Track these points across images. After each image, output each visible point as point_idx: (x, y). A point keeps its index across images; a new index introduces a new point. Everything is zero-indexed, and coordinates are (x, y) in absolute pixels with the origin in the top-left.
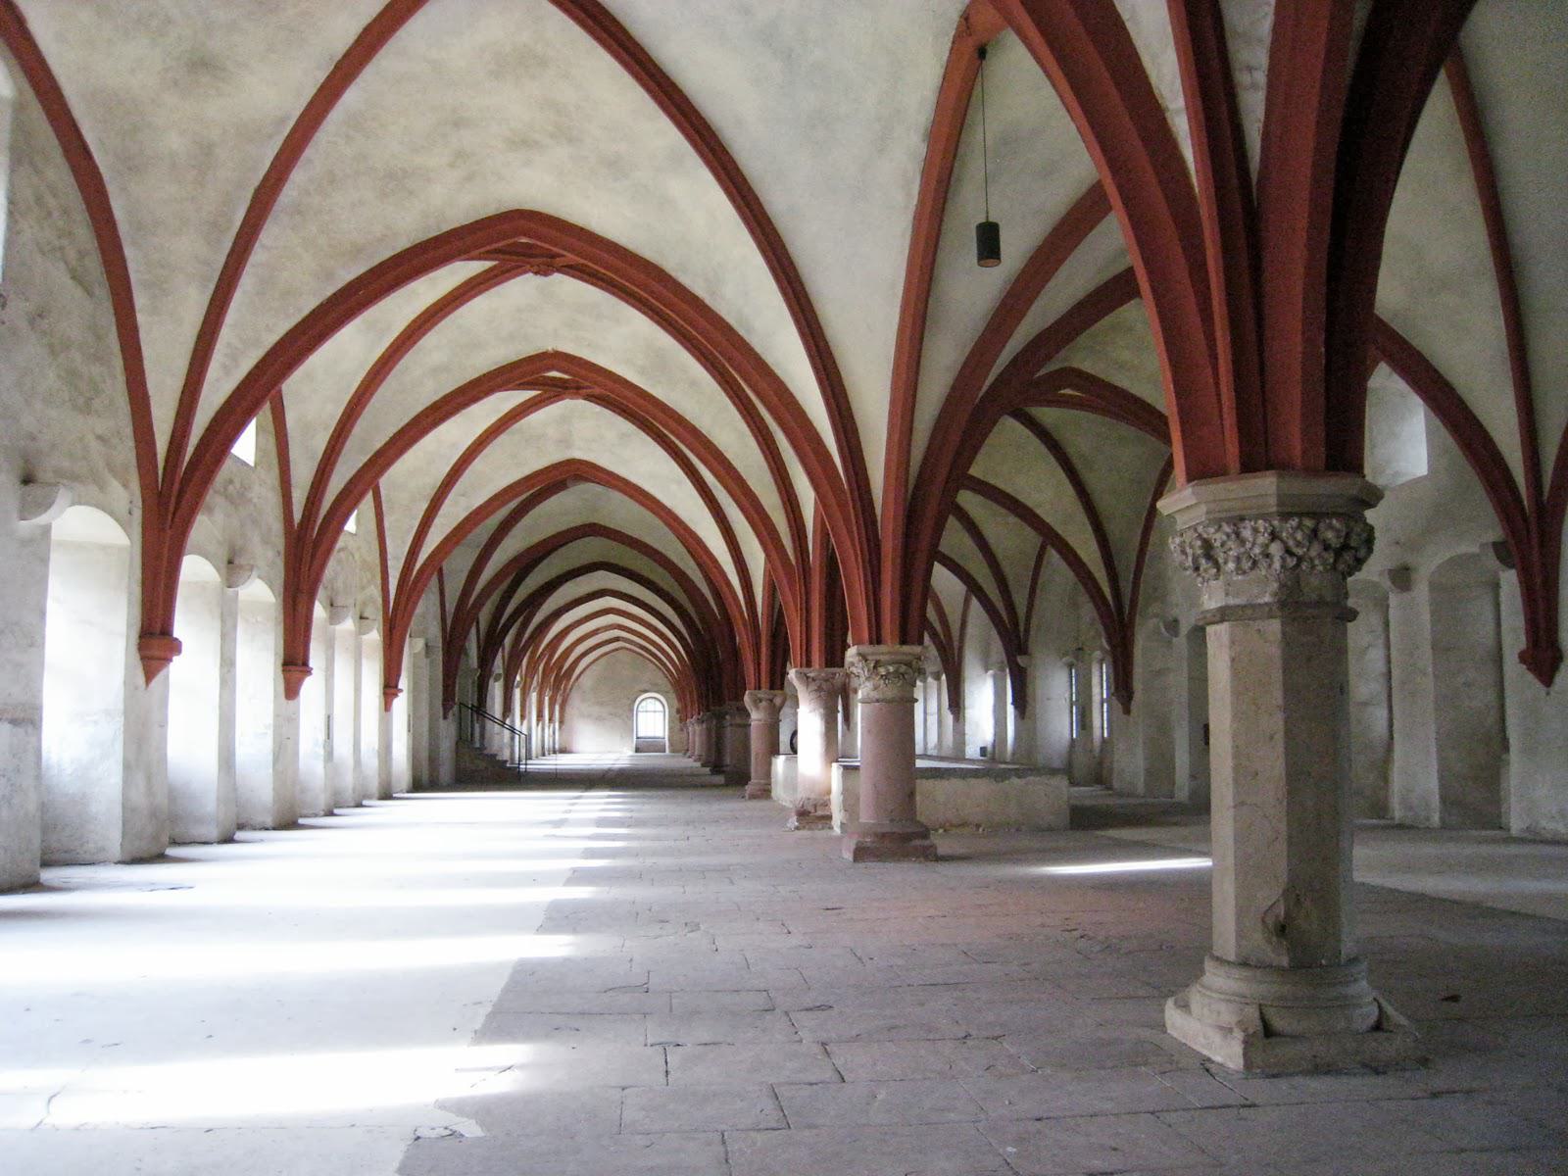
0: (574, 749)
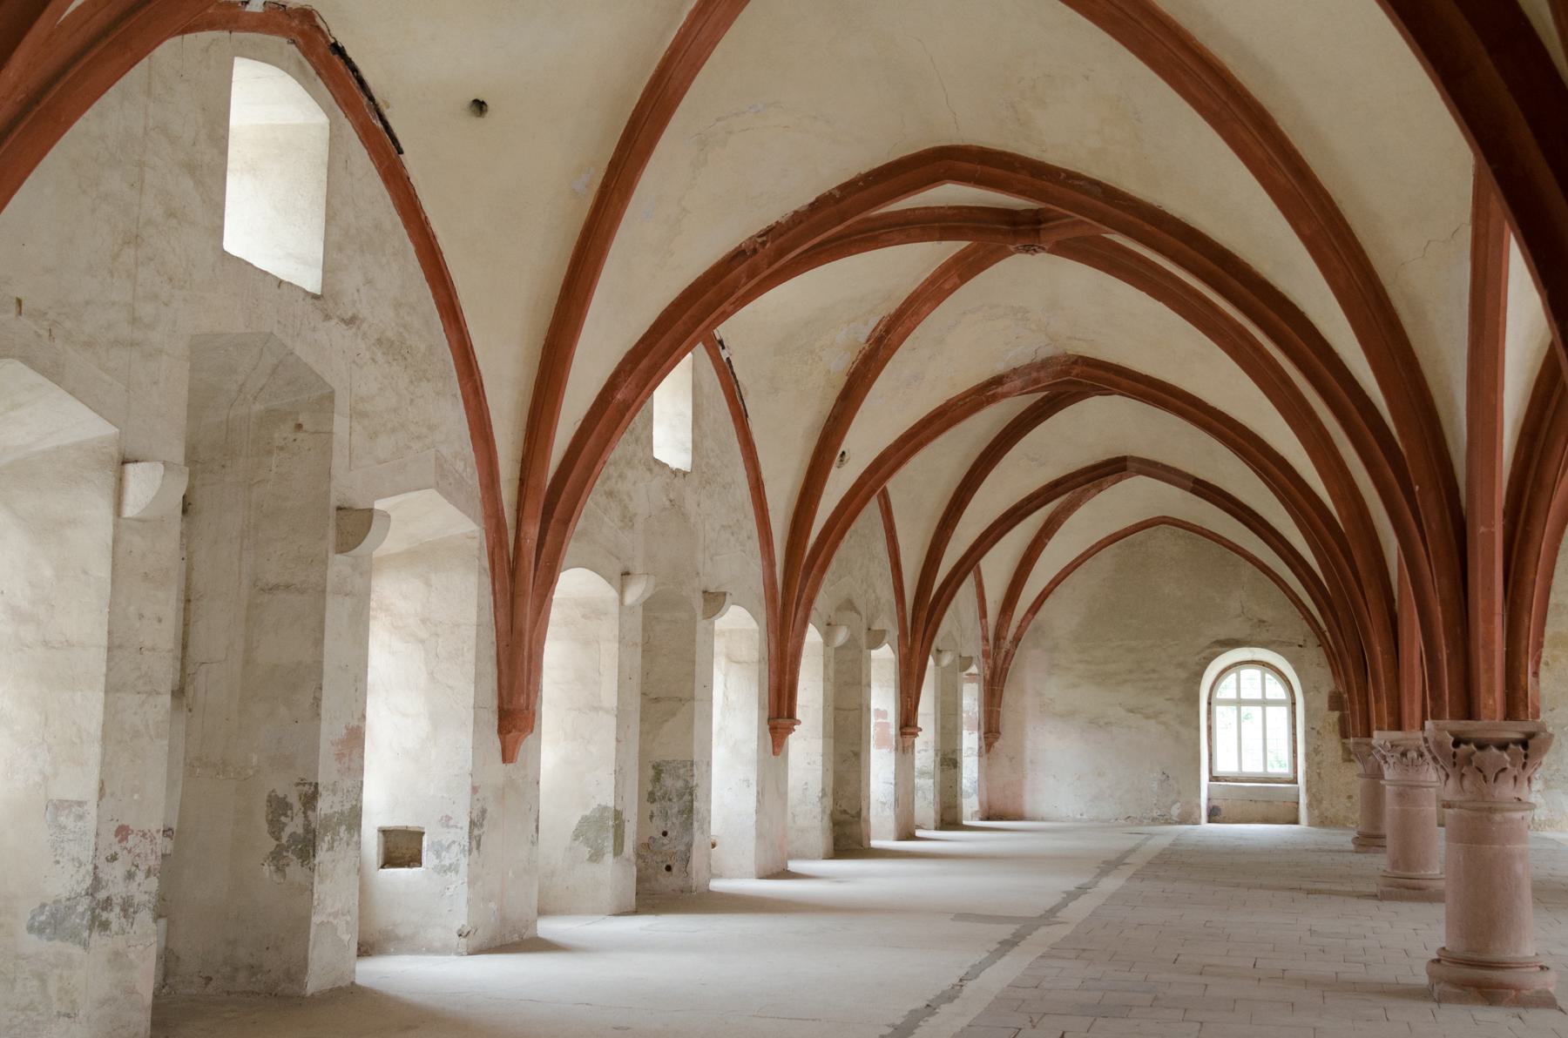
0: (1029, 803)
